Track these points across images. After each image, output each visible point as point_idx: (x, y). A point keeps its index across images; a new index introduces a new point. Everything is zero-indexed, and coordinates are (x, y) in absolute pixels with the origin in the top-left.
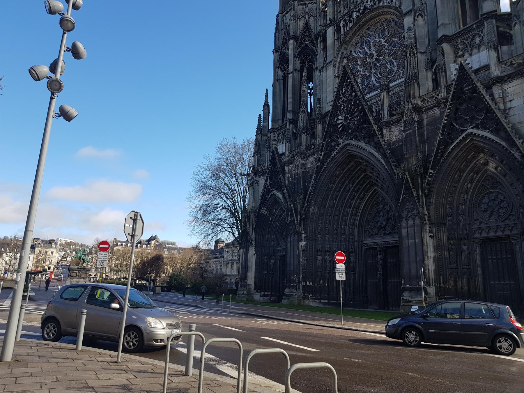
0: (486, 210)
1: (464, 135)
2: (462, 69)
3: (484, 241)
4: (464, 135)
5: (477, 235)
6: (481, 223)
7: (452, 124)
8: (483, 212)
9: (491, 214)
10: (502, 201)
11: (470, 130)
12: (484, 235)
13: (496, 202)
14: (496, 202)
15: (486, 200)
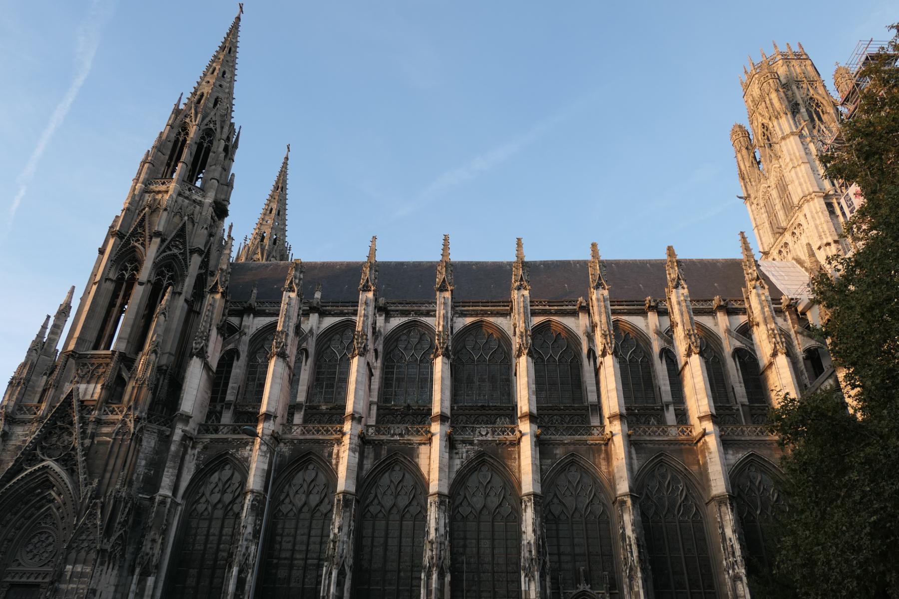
0: (31, 551)
1: (40, 465)
2: (70, 395)
3: (13, 585)
4: (40, 465)
5: (9, 579)
6: (19, 564)
7: (35, 450)
8: (28, 553)
9: (34, 556)
10: (51, 544)
11: (49, 462)
12: (16, 579)
13: (44, 544)
14: (44, 544)
15: (36, 540)
